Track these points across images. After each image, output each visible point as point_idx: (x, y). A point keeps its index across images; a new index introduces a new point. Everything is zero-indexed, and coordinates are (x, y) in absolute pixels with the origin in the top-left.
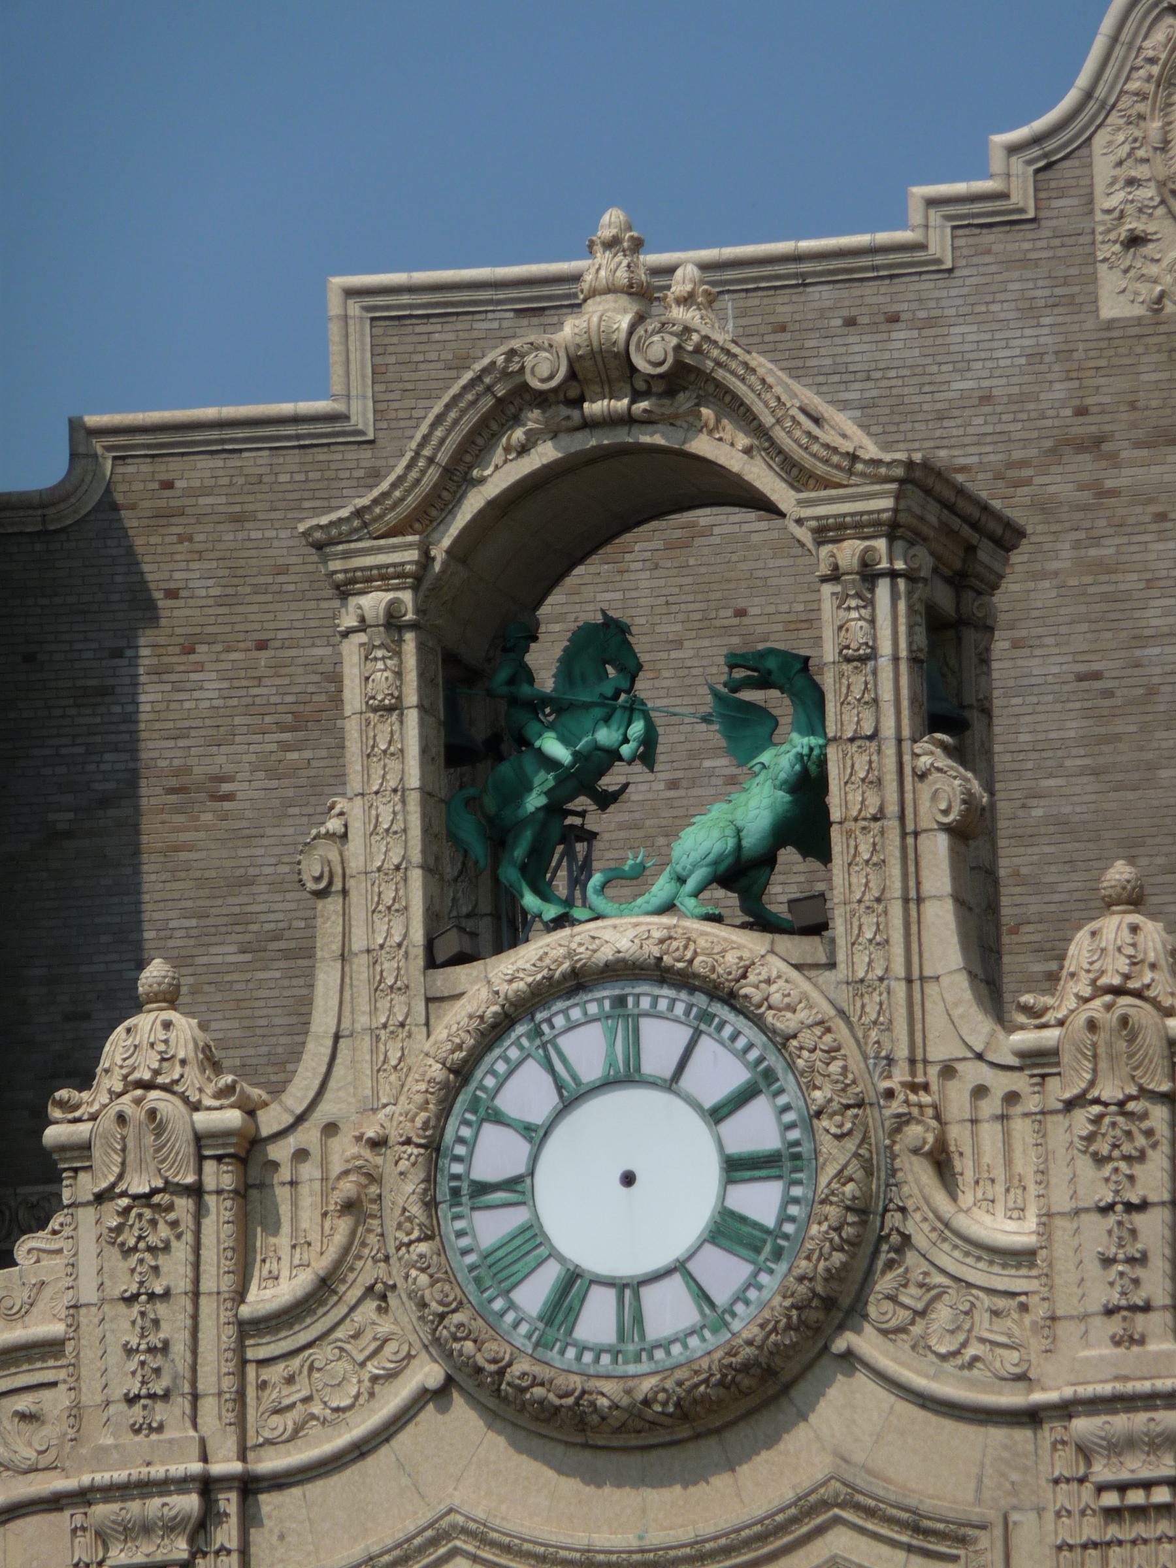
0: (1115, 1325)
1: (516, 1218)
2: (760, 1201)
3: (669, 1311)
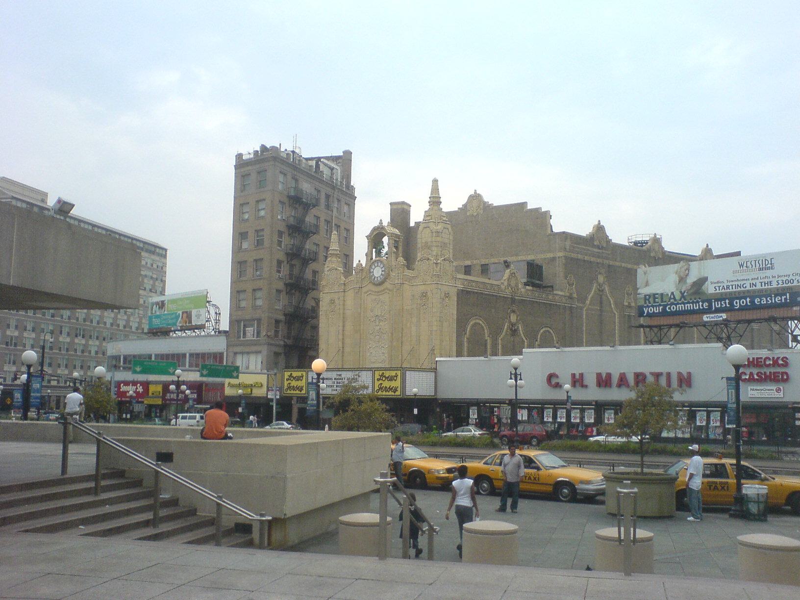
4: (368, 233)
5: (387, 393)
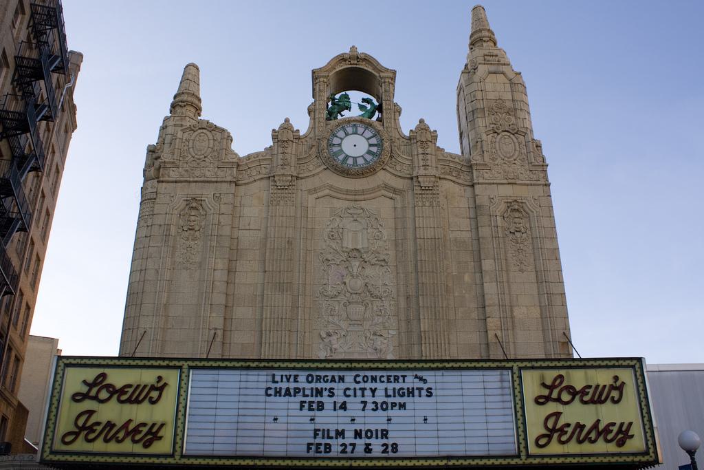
0: (424, 168)
1: (339, 148)
2: (374, 149)
3: (360, 161)
4: (321, 62)
5: (587, 448)
